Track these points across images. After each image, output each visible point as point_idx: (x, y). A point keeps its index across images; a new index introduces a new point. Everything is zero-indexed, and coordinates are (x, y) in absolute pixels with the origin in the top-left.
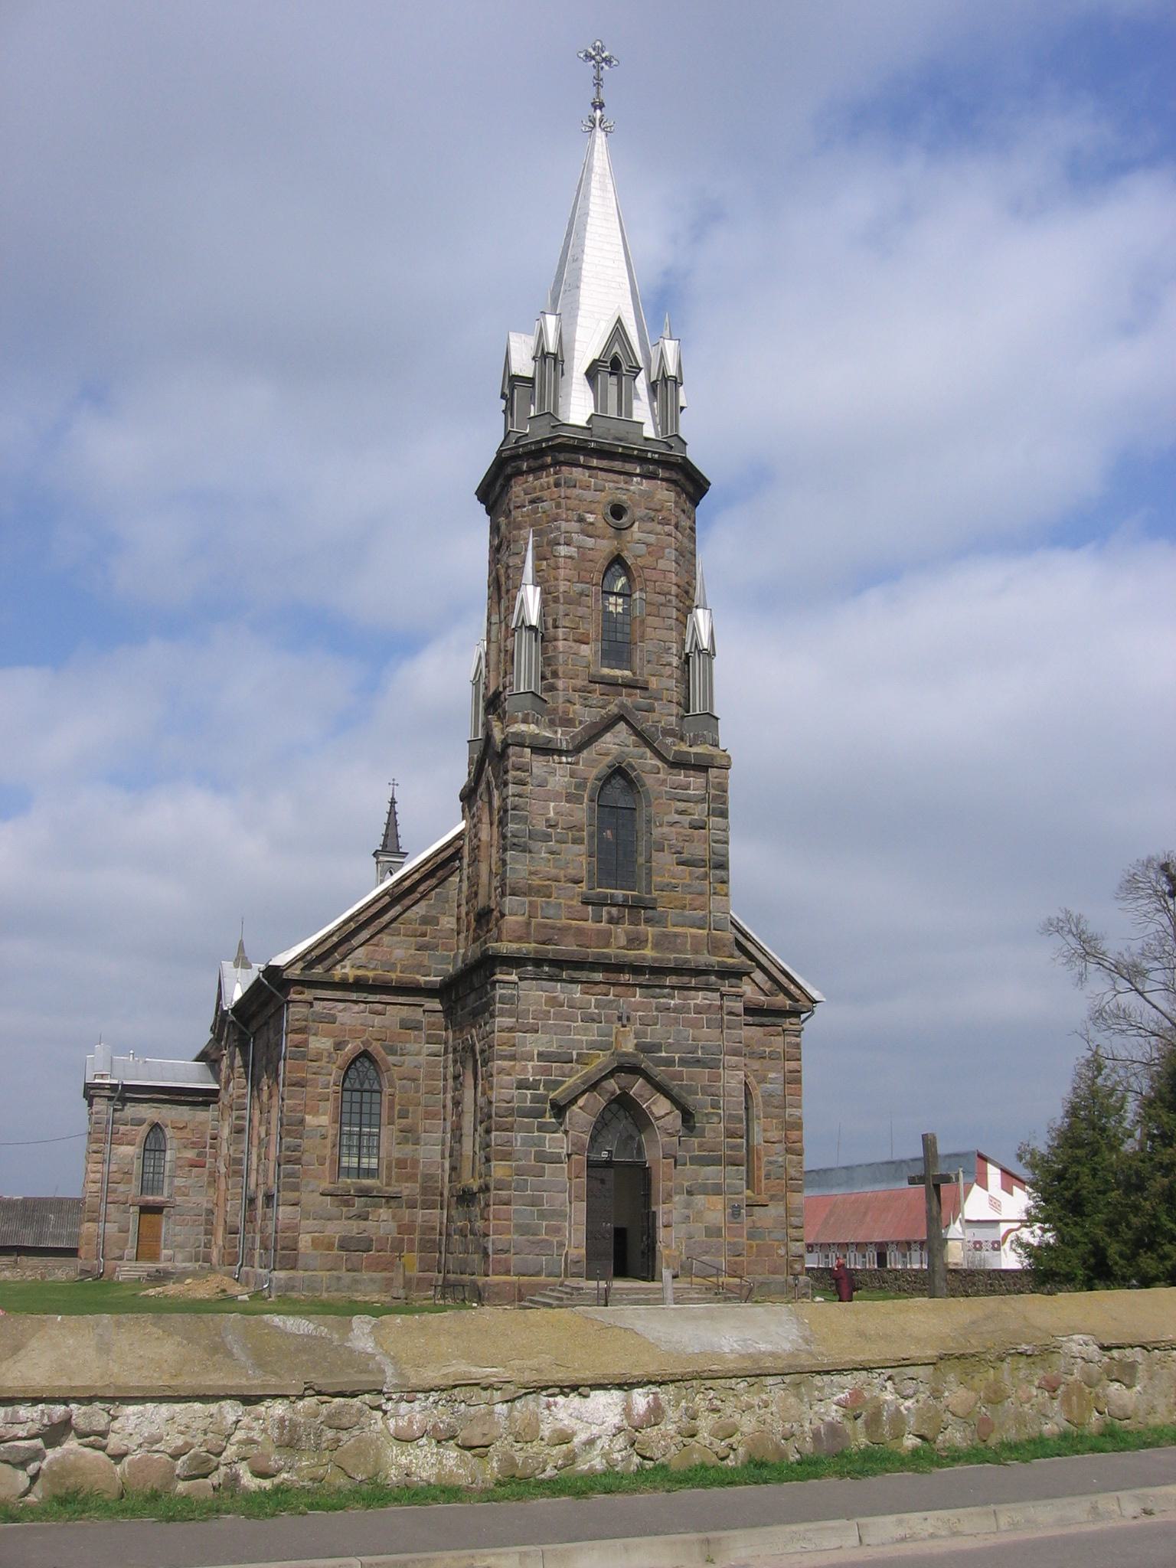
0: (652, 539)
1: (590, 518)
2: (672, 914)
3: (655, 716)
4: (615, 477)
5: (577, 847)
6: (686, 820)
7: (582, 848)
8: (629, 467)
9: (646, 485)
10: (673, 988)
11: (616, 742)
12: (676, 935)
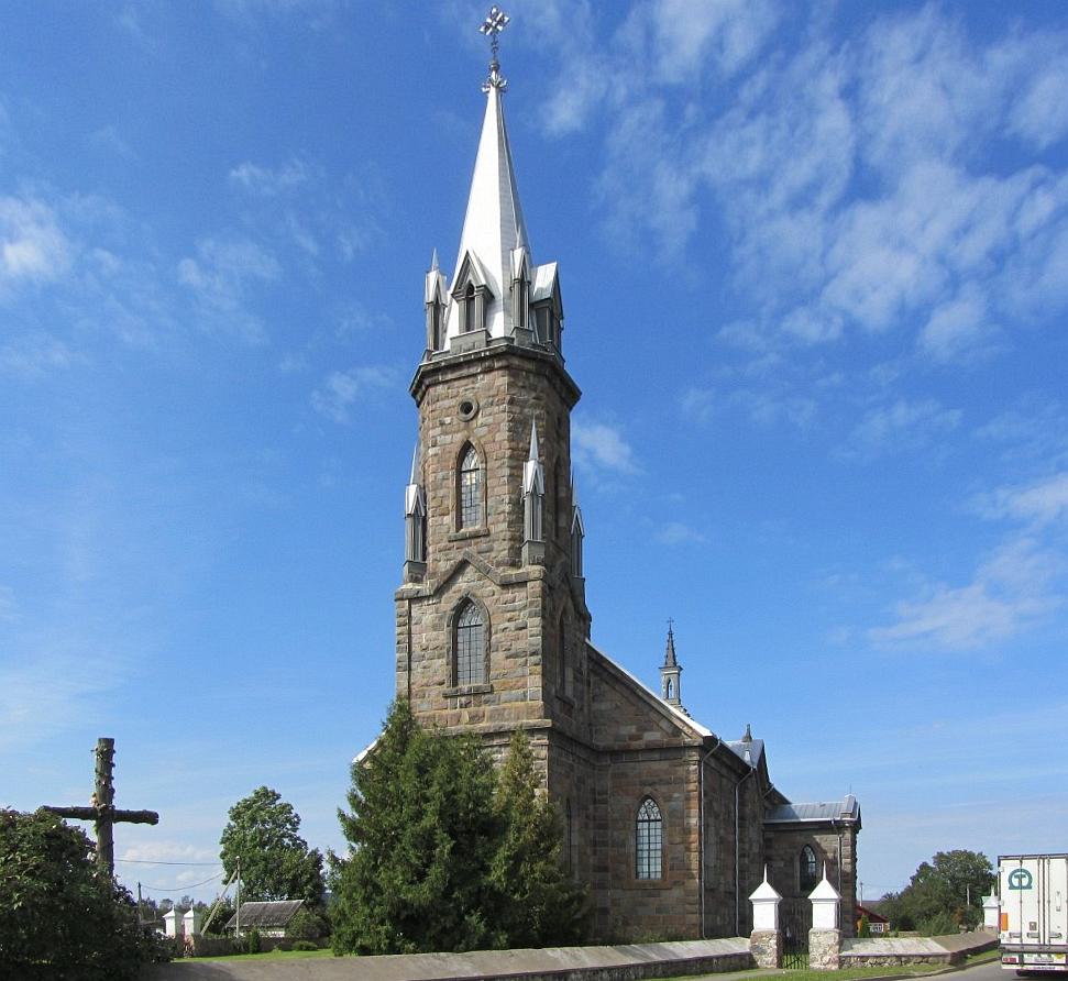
0: (490, 420)
1: (448, 420)
2: (504, 695)
3: (493, 555)
4: (463, 382)
5: (440, 661)
6: (512, 625)
7: (444, 660)
8: (473, 370)
9: (487, 378)
10: (500, 746)
11: (462, 584)
12: (504, 709)
